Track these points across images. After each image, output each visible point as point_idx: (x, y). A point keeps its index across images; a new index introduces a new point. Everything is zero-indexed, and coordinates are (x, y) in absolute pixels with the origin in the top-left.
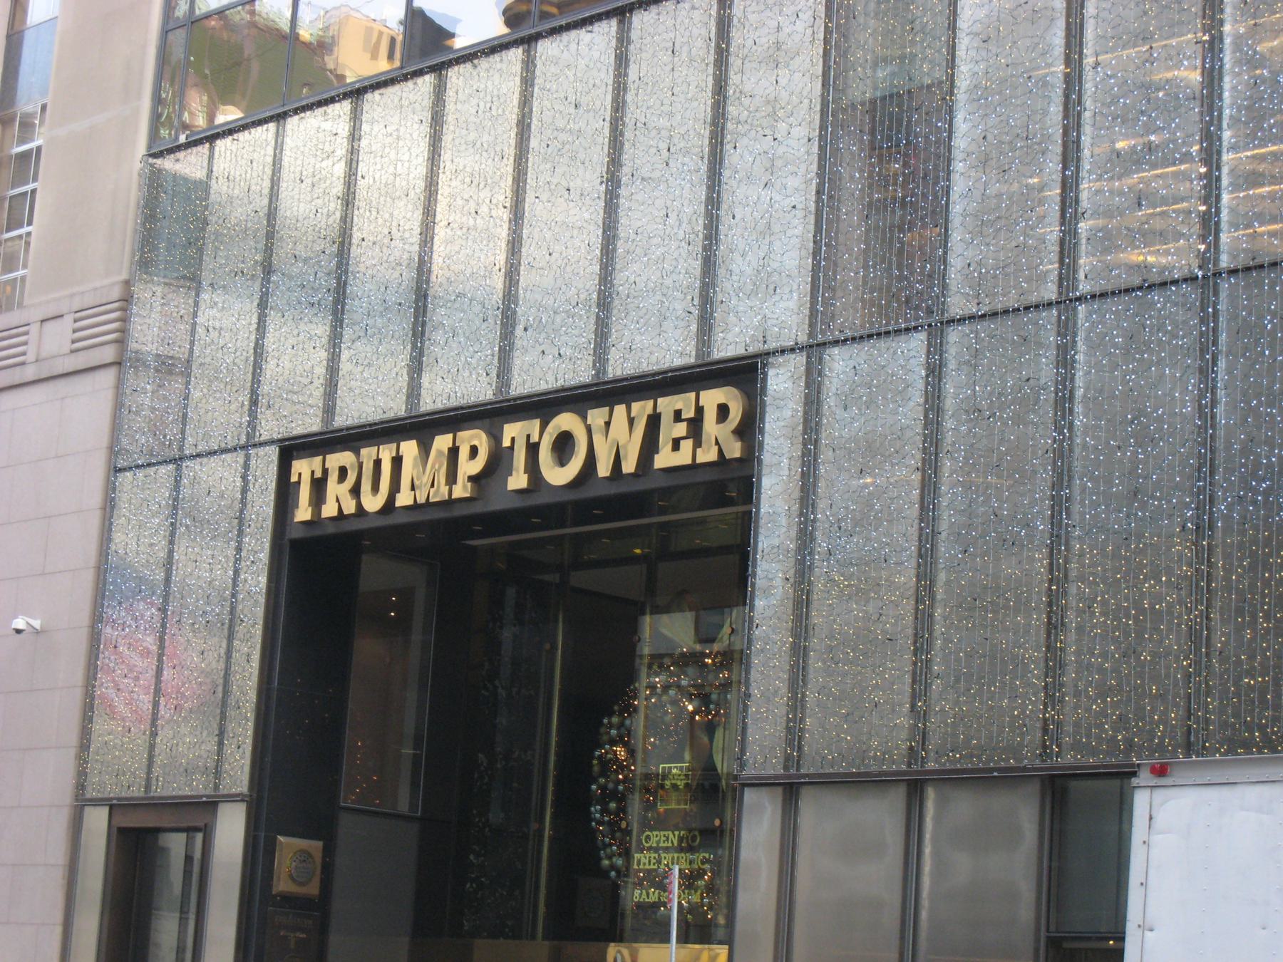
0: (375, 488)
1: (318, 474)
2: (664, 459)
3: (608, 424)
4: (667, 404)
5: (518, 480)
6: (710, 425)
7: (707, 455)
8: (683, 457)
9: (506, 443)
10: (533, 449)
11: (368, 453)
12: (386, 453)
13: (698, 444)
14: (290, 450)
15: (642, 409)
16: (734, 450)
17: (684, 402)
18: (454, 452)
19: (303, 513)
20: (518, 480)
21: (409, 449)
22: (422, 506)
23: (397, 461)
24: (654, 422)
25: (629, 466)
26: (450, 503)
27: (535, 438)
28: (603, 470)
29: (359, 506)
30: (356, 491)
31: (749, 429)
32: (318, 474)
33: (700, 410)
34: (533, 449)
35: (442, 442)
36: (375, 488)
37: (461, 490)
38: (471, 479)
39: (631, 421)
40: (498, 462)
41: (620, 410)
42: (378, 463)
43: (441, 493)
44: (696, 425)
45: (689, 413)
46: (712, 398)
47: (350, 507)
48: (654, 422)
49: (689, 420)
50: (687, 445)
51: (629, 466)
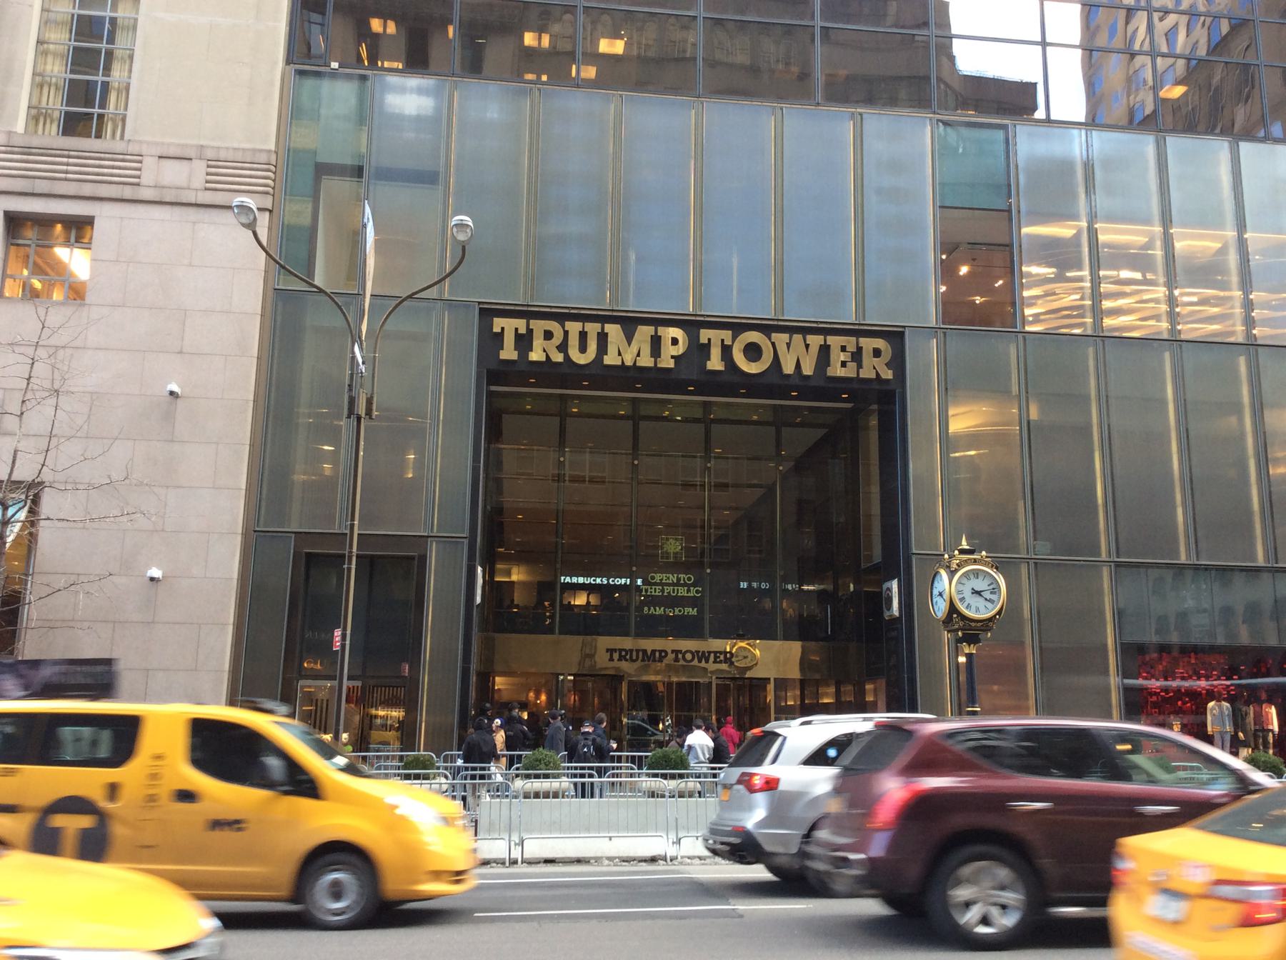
0: (583, 349)
1: (523, 331)
2: (836, 370)
3: (788, 345)
4: (835, 341)
5: (715, 363)
6: (867, 359)
7: (867, 373)
8: (849, 372)
9: (703, 340)
10: (726, 351)
11: (574, 327)
12: (593, 328)
13: (860, 366)
14: (487, 313)
15: (815, 341)
16: (888, 374)
17: (850, 342)
18: (656, 342)
19: (509, 352)
20: (715, 363)
21: (613, 330)
22: (628, 367)
23: (603, 337)
24: (825, 350)
25: (808, 370)
26: (656, 369)
27: (728, 342)
28: (788, 368)
29: (567, 357)
30: (563, 347)
31: (898, 362)
32: (523, 331)
33: (860, 349)
34: (726, 351)
35: (644, 332)
36: (583, 349)
37: (667, 362)
38: (673, 357)
39: (807, 346)
40: (700, 350)
41: (797, 338)
42: (583, 335)
43: (646, 361)
44: (857, 356)
45: (852, 348)
46: (868, 344)
47: (558, 357)
48: (825, 350)
49: (853, 353)
50: (852, 366)
51: (808, 370)
